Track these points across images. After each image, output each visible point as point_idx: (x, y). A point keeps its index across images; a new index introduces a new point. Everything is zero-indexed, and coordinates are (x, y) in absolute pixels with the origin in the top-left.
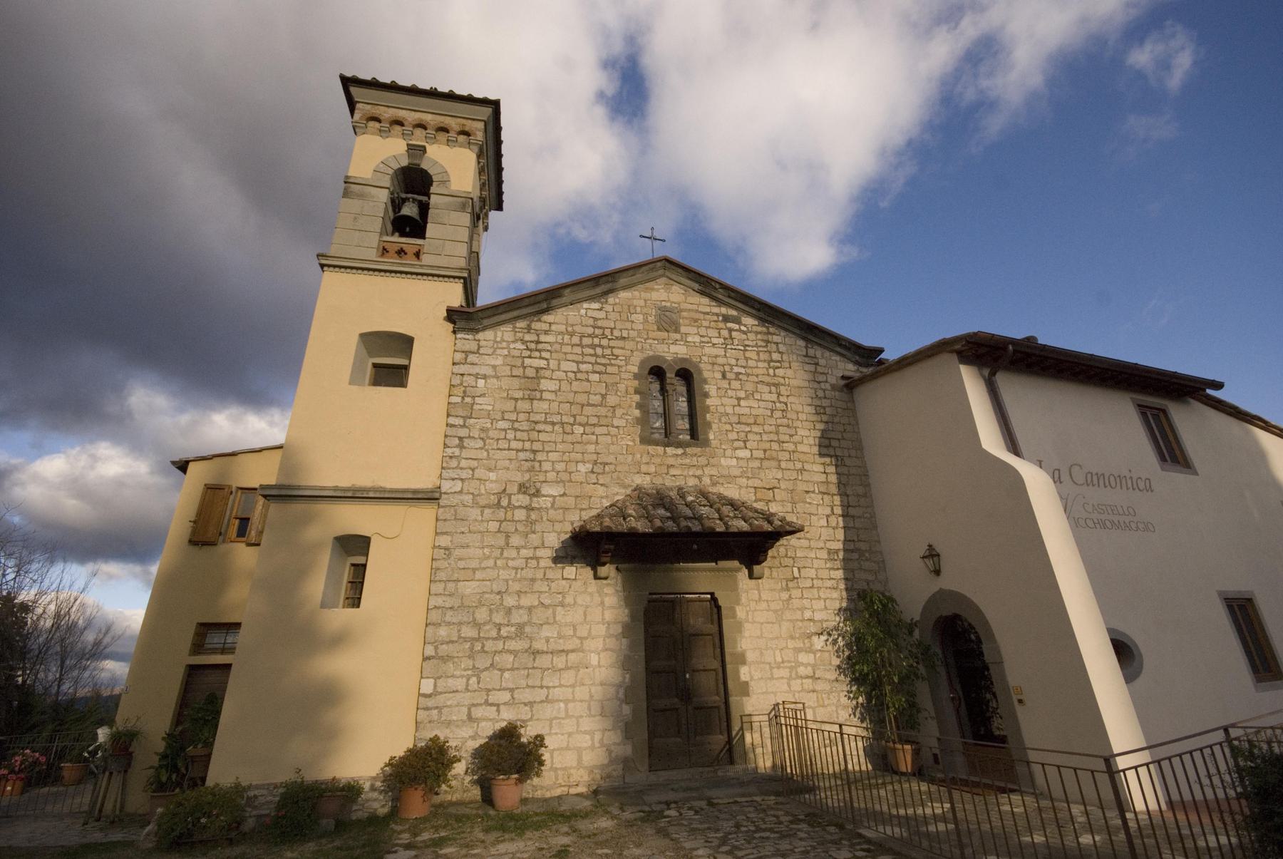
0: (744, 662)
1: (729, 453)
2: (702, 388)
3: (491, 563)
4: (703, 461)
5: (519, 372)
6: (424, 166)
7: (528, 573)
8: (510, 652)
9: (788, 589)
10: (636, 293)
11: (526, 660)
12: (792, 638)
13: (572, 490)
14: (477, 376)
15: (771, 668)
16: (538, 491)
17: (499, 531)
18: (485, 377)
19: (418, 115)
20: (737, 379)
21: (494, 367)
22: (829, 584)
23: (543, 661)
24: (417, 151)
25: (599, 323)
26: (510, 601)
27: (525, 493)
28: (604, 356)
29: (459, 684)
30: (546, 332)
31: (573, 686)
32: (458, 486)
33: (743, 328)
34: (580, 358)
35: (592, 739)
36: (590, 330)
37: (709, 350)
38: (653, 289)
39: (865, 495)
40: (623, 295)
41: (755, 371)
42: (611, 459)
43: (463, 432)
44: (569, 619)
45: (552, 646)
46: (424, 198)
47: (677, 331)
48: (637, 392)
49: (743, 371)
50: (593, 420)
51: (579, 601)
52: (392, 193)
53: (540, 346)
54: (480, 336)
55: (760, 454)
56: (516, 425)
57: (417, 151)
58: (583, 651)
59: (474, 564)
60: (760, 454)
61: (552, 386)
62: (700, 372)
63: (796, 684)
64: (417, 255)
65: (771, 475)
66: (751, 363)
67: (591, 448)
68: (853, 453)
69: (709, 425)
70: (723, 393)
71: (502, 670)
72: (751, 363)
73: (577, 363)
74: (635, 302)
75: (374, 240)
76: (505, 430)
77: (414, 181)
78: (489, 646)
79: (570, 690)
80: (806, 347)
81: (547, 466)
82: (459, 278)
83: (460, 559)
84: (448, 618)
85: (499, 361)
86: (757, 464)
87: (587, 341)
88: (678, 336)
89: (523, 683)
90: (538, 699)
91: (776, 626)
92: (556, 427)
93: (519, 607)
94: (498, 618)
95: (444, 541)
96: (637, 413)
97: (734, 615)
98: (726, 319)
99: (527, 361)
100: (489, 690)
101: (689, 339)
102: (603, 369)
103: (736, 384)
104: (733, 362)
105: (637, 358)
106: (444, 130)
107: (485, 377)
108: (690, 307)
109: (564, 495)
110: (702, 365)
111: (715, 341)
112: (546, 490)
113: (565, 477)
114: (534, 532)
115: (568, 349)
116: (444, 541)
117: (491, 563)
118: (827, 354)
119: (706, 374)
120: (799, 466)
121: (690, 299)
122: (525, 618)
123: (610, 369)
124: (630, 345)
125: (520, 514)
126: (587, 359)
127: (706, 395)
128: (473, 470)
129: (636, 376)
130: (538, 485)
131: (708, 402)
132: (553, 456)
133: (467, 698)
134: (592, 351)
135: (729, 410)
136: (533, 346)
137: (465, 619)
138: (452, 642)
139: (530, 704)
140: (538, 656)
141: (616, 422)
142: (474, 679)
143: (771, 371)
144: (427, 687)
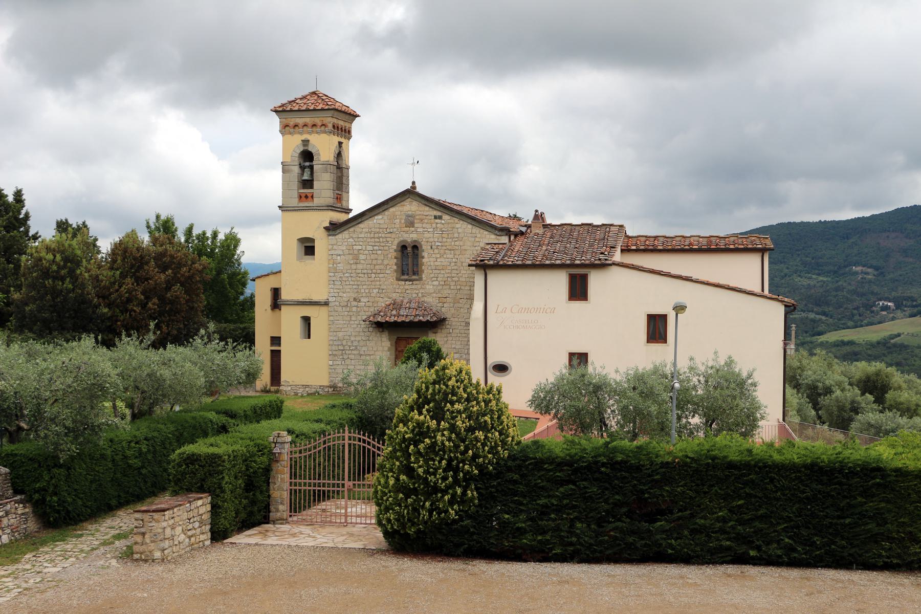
4: (419, 286)
5: (351, 252)
7: (357, 330)
13: (371, 300)
24: (306, 142)
26: (352, 339)
40: (392, 210)
43: (334, 279)
57: (306, 142)
65: (446, 292)
66: (444, 240)
67: (378, 283)
69: (423, 271)
70: (430, 256)
72: (444, 240)
81: (363, 291)
86: (440, 287)
87: (376, 235)
88: (413, 229)
94: (349, 344)
95: (331, 318)
96: (395, 267)
98: (436, 217)
103: (436, 251)
105: (396, 242)
106: (314, 125)
116: (331, 318)
119: (424, 247)
123: (386, 248)
124: (393, 236)
125: (354, 309)
127: (423, 257)
131: (424, 260)
133: (342, 367)
135: (432, 264)
144: (331, 363)
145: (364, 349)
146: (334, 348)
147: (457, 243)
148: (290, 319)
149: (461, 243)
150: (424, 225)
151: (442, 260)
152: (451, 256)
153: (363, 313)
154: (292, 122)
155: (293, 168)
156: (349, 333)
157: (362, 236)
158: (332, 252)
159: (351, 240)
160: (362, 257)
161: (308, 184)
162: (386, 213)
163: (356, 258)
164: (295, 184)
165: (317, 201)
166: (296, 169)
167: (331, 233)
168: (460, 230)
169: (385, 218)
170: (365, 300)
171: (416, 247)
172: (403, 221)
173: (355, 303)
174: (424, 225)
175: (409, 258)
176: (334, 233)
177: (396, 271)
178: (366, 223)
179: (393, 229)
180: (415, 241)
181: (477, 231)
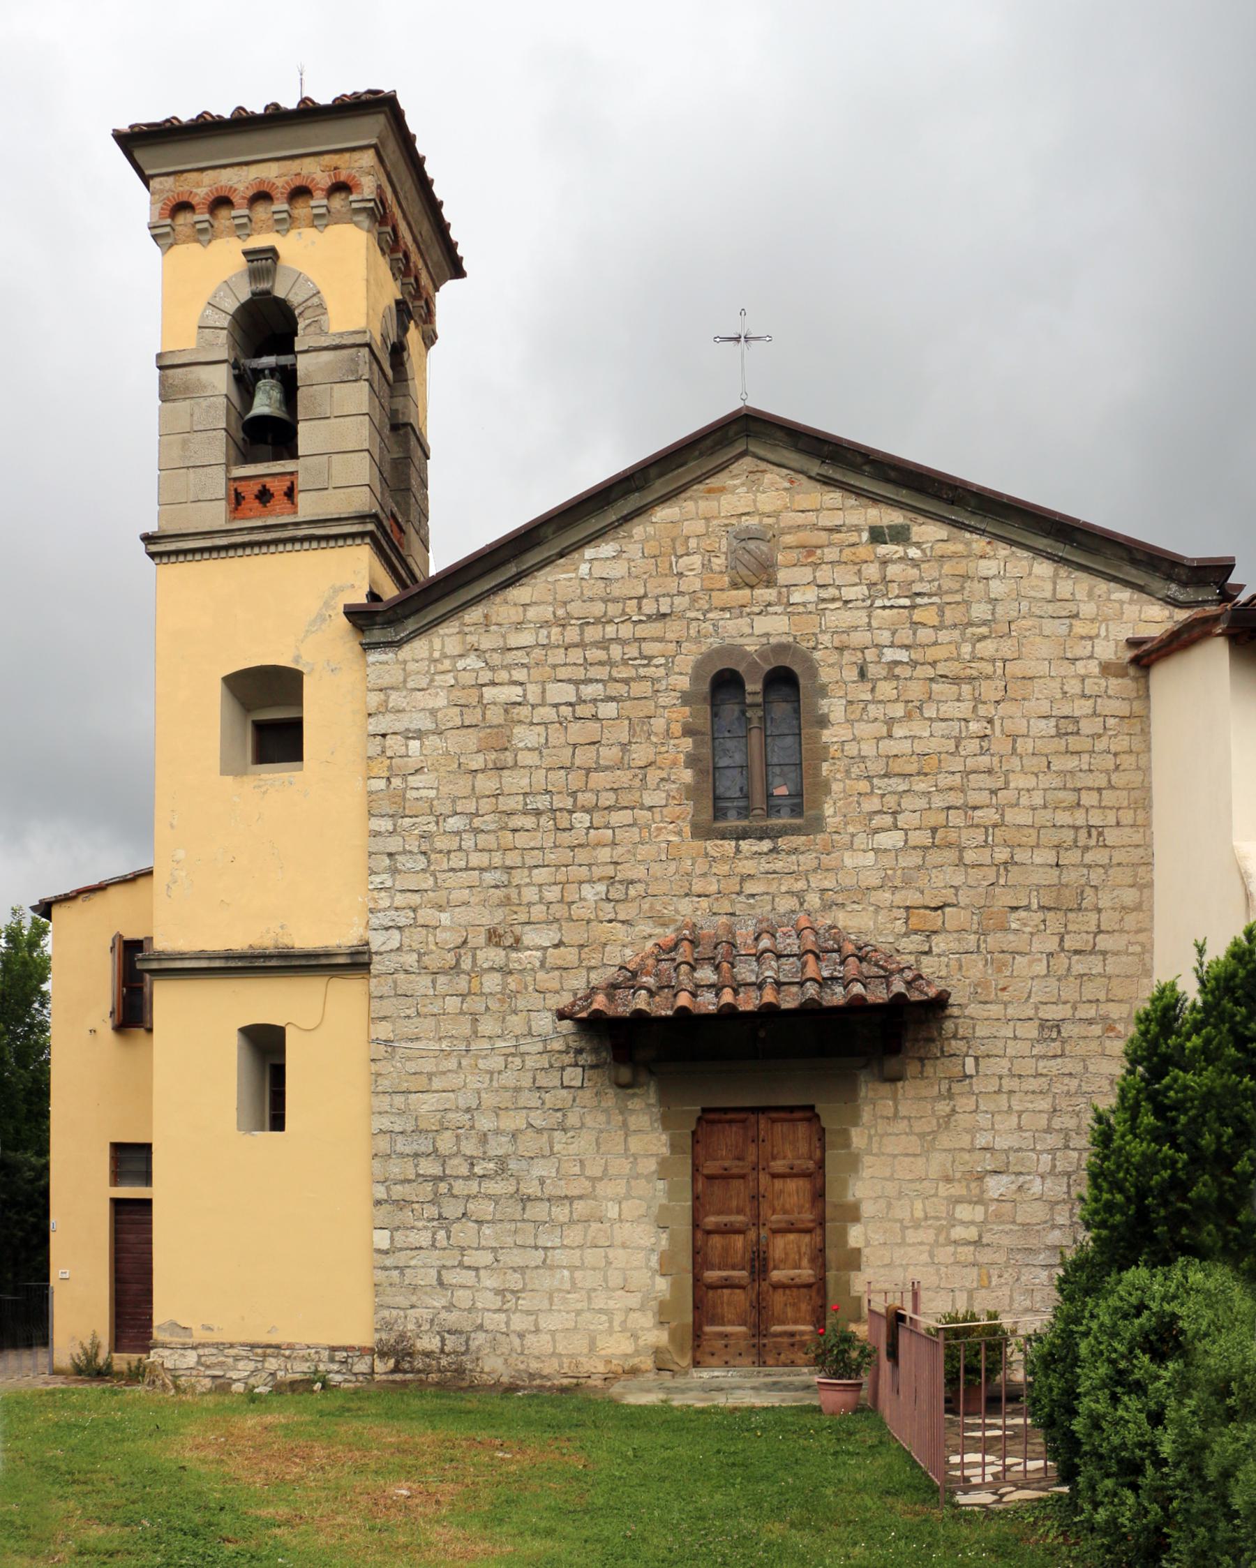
0: (856, 1219)
1: (861, 840)
2: (815, 706)
3: (452, 1064)
4: (808, 861)
5: (473, 717)
6: (280, 292)
7: (508, 1079)
8: (489, 1197)
9: (950, 1096)
10: (690, 505)
11: (514, 1210)
12: (948, 1180)
13: (574, 935)
14: (408, 735)
15: (904, 1228)
16: (518, 940)
17: (462, 1013)
18: (420, 735)
19: (254, 173)
21: (433, 712)
22: (1033, 1084)
23: (537, 1211)
24: (263, 262)
25: (616, 590)
26: (485, 1123)
27: (497, 945)
28: (625, 662)
29: (424, 1239)
30: (519, 626)
32: (395, 939)
33: (913, 552)
34: (580, 673)
35: (611, 1321)
36: (598, 609)
37: (837, 618)
38: (722, 490)
39: (1138, 908)
40: (663, 514)
41: (932, 654)
42: (638, 872)
43: (394, 844)
44: (573, 1149)
45: (549, 1190)
46: (285, 360)
47: (770, 583)
48: (688, 731)
49: (903, 655)
50: (608, 799)
51: (588, 1120)
52: (235, 366)
53: (510, 657)
54: (406, 652)
56: (477, 822)
57: (263, 262)
58: (595, 1198)
59: (428, 1065)
60: (923, 838)
62: (813, 671)
63: (944, 1255)
64: (290, 493)
65: (944, 879)
66: (924, 635)
67: (604, 854)
68: (1127, 817)
69: (824, 787)
71: (480, 1222)
72: (924, 635)
73: (577, 683)
74: (689, 528)
75: (216, 482)
76: (458, 833)
77: (266, 327)
78: (459, 1187)
79: (578, 1252)
81: (530, 894)
82: (362, 535)
83: (409, 1059)
84: (399, 1147)
85: (441, 701)
86: (914, 859)
87: (593, 633)
88: (769, 594)
89: (509, 1241)
90: (533, 1264)
91: (921, 1161)
92: (543, 819)
93: (497, 1132)
94: (469, 1148)
95: (383, 1030)
96: (687, 776)
97: (847, 1144)
98: (877, 535)
99: (489, 693)
100: (463, 1249)
101: (796, 597)
102: (621, 689)
103: (886, 689)
104: (885, 637)
105: (687, 661)
106: (300, 192)
107: (420, 735)
108: (801, 519)
110: (817, 655)
111: (848, 593)
112: (531, 937)
113: (559, 911)
114: (515, 1012)
115: (558, 656)
117: (452, 1064)
118: (1102, 586)
119: (826, 675)
120: (1002, 855)
121: (804, 501)
123: (638, 689)
124: (673, 629)
125: (492, 982)
126: (594, 672)
127: (823, 722)
128: (414, 910)
129: (686, 699)
131: (827, 735)
132: (541, 875)
133: (434, 1258)
134: (600, 655)
135: (868, 749)
136: (496, 659)
137: (423, 1149)
138: (409, 1181)
139: (521, 1270)
140: (529, 1204)
141: (648, 801)
142: (442, 1233)
144: (382, 1239)
146: (396, 1169)
149: (1007, 648)
150: (824, 575)
152: (964, 709)
153: (536, 1001)
155: (204, 373)
157: (526, 638)
159: (472, 662)
160: (525, 736)
161: (269, 437)
162: (638, 529)
163: (498, 744)
164: (215, 447)
165: (308, 506)
166: (220, 380)
167: (377, 635)
168: (997, 588)
169: (634, 550)
170: (545, 937)
171: (784, 680)
172: (719, 562)
173: (494, 956)
174: (824, 575)
176: (390, 634)
180: (782, 648)
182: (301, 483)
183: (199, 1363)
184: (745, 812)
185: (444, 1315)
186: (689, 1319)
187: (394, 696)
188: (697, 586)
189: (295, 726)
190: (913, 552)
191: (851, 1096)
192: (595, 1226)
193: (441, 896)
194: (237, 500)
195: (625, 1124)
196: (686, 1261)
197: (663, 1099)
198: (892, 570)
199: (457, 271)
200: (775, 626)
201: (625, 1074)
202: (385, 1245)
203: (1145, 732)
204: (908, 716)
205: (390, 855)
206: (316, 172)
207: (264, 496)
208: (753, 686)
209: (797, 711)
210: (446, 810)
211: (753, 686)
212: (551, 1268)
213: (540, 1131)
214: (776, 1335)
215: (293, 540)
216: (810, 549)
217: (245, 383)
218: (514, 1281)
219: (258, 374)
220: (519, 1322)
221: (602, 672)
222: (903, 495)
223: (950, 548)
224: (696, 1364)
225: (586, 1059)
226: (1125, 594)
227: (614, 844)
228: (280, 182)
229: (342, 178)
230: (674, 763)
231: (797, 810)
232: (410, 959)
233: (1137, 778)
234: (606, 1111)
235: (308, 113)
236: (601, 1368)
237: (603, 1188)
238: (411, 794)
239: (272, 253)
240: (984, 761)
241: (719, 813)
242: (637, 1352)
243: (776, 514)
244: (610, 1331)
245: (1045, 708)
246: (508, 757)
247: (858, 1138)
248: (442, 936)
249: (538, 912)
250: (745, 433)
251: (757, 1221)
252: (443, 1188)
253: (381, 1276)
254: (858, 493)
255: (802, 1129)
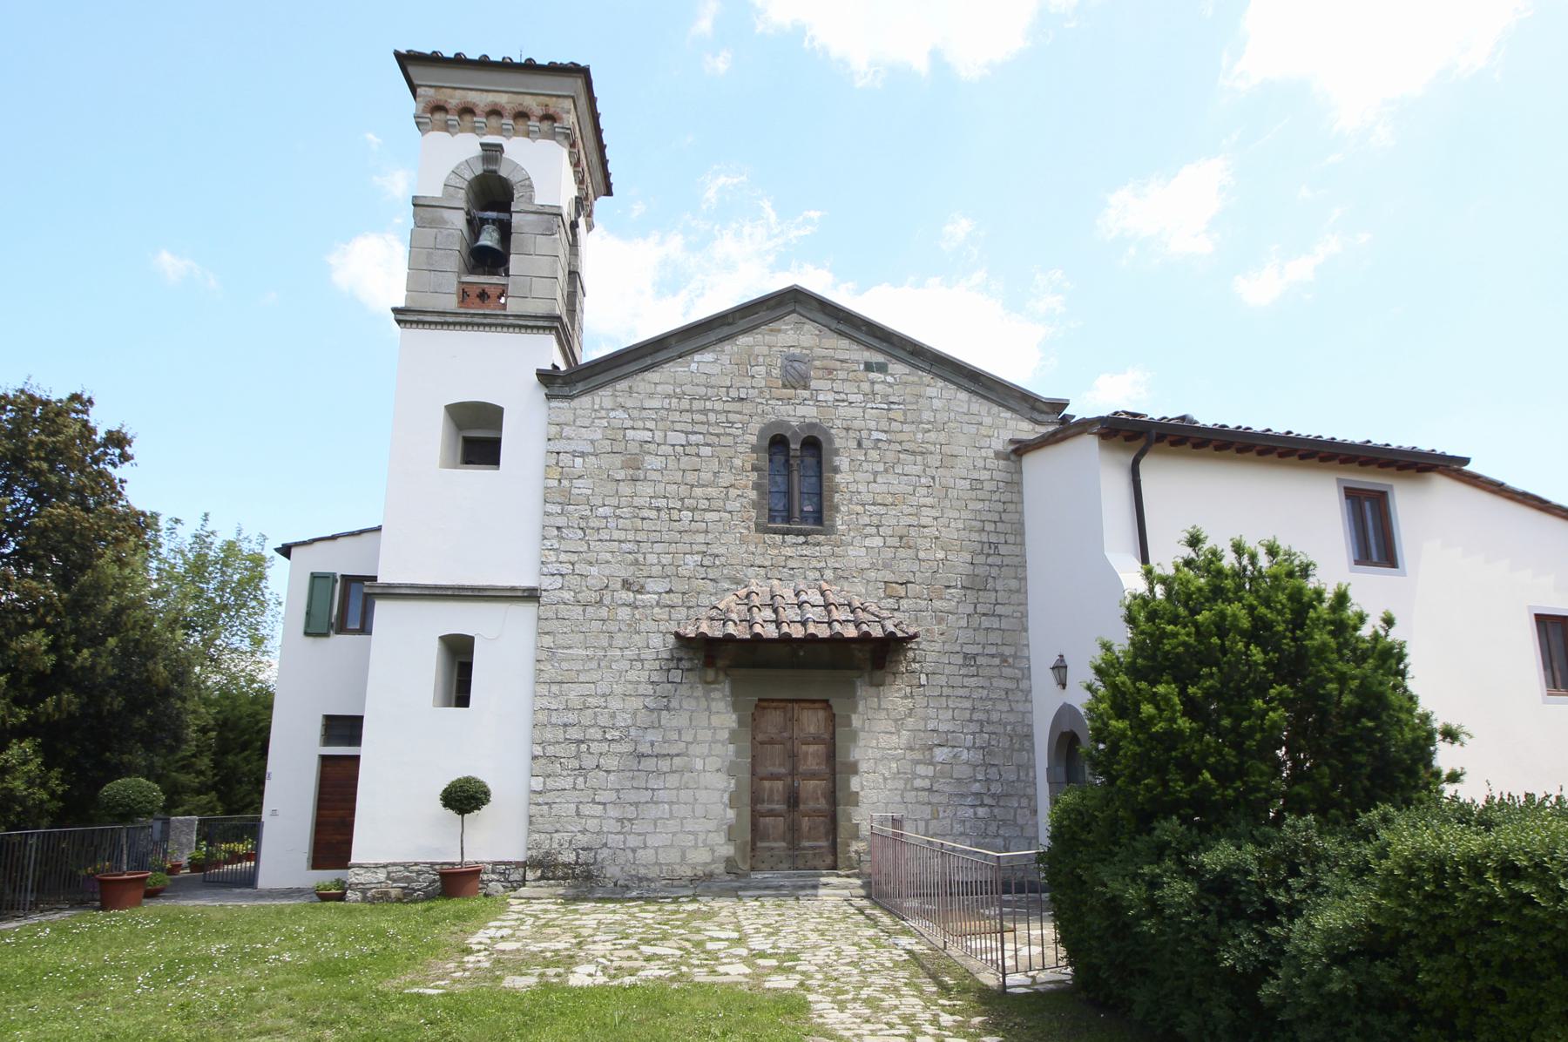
0: (856, 772)
2: (831, 461)
3: (594, 665)
4: (826, 549)
6: (503, 173)
7: (632, 676)
12: (911, 749)
14: (574, 454)
15: (885, 779)
16: (642, 587)
18: (583, 455)
19: (490, 98)
20: (876, 448)
21: (592, 442)
22: (961, 692)
23: (649, 764)
24: (492, 153)
25: (713, 381)
26: (615, 704)
29: (567, 783)
30: (651, 395)
31: (677, 789)
32: (558, 581)
33: (890, 379)
36: (702, 391)
37: (844, 411)
38: (779, 331)
39: (1018, 591)
40: (743, 340)
41: (900, 437)
42: (722, 550)
43: (561, 521)
44: (674, 723)
45: (657, 750)
47: (806, 387)
48: (754, 469)
49: (883, 436)
50: (704, 504)
51: (685, 706)
52: (468, 213)
53: (645, 414)
54: (576, 403)
55: (895, 541)
56: (618, 512)
57: (492, 153)
61: (658, 463)
62: (830, 440)
63: (910, 796)
67: (701, 538)
68: (1011, 539)
69: (836, 509)
73: (687, 433)
74: (757, 350)
75: (451, 282)
77: (492, 195)
78: (595, 747)
80: (969, 401)
81: (652, 558)
82: (550, 328)
84: (554, 720)
85: (598, 435)
86: (889, 553)
87: (697, 405)
88: (806, 394)
92: (662, 514)
93: (623, 710)
94: (603, 721)
95: (547, 641)
96: (753, 495)
97: (850, 725)
98: (869, 367)
99: (630, 433)
101: (821, 397)
103: (874, 454)
104: (872, 425)
105: (755, 427)
106: (522, 115)
107: (583, 455)
109: (670, 591)
111: (852, 398)
112: (651, 585)
113: (670, 570)
115: (676, 416)
116: (547, 641)
117: (594, 665)
118: (995, 409)
119: (838, 443)
120: (940, 555)
122: (629, 722)
124: (747, 408)
125: (624, 613)
126: (697, 428)
127: (836, 470)
129: (754, 449)
130: (642, 581)
131: (838, 478)
132: (658, 548)
135: (862, 488)
136: (635, 413)
139: (636, 804)
141: (729, 508)
142: (581, 779)
143: (920, 436)
144: (537, 784)
145: (651, 736)
147: (932, 436)
148: (404, 644)
149: (942, 437)
150: (837, 386)
151: (891, 478)
152: (917, 469)
153: (653, 626)
154: (455, 99)
155: (447, 214)
156: (603, 688)
157: (656, 403)
158: (559, 445)
159: (620, 414)
160: (652, 462)
161: (488, 260)
162: (728, 347)
163: (633, 463)
164: (452, 261)
166: (458, 220)
167: (556, 391)
168: (937, 404)
169: (725, 359)
170: (661, 586)
171: (814, 445)
172: (776, 372)
173: (628, 596)
174: (837, 386)
175: (796, 477)
177: (755, 505)
178: (669, 369)
179: (744, 391)
180: (812, 426)
181: (979, 407)
182: (510, 291)
183: (388, 878)
184: (788, 519)
185: (580, 836)
186: (749, 838)
187: (567, 429)
188: (763, 384)
189: (496, 443)
190: (890, 379)
191: (851, 695)
192: (687, 775)
193: (591, 556)
194: (464, 295)
195: (708, 708)
196: (747, 798)
197: (733, 693)
198: (877, 387)
199: (609, 192)
200: (809, 412)
201: (711, 674)
202: (539, 788)
203: (1020, 493)
204: (886, 471)
205: (558, 528)
206: (531, 103)
207: (483, 296)
208: (795, 446)
209: (819, 463)
210: (599, 502)
211: (795, 446)
212: (656, 803)
213: (652, 710)
214: (805, 848)
215: (502, 326)
216: (830, 371)
217: (475, 226)
218: (630, 812)
219: (484, 221)
220: (633, 841)
221: (703, 429)
222: (884, 346)
223: (911, 379)
224: (753, 869)
225: (685, 664)
226: (1008, 414)
227: (707, 532)
228: (508, 107)
229: (551, 111)
230: (746, 487)
231: (819, 519)
232: (568, 596)
233: (1015, 517)
234: (697, 698)
235: (530, 67)
236: (689, 873)
237: (694, 749)
238: (575, 491)
239: (499, 148)
240: (929, 501)
241: (772, 519)
242: (713, 861)
243: (811, 349)
244: (696, 847)
245: (964, 473)
246: (641, 474)
247: (856, 721)
248: (590, 581)
249: (656, 570)
250: (793, 301)
251: (793, 772)
252: (583, 747)
253: (534, 810)
254: (858, 342)
255: (821, 714)
